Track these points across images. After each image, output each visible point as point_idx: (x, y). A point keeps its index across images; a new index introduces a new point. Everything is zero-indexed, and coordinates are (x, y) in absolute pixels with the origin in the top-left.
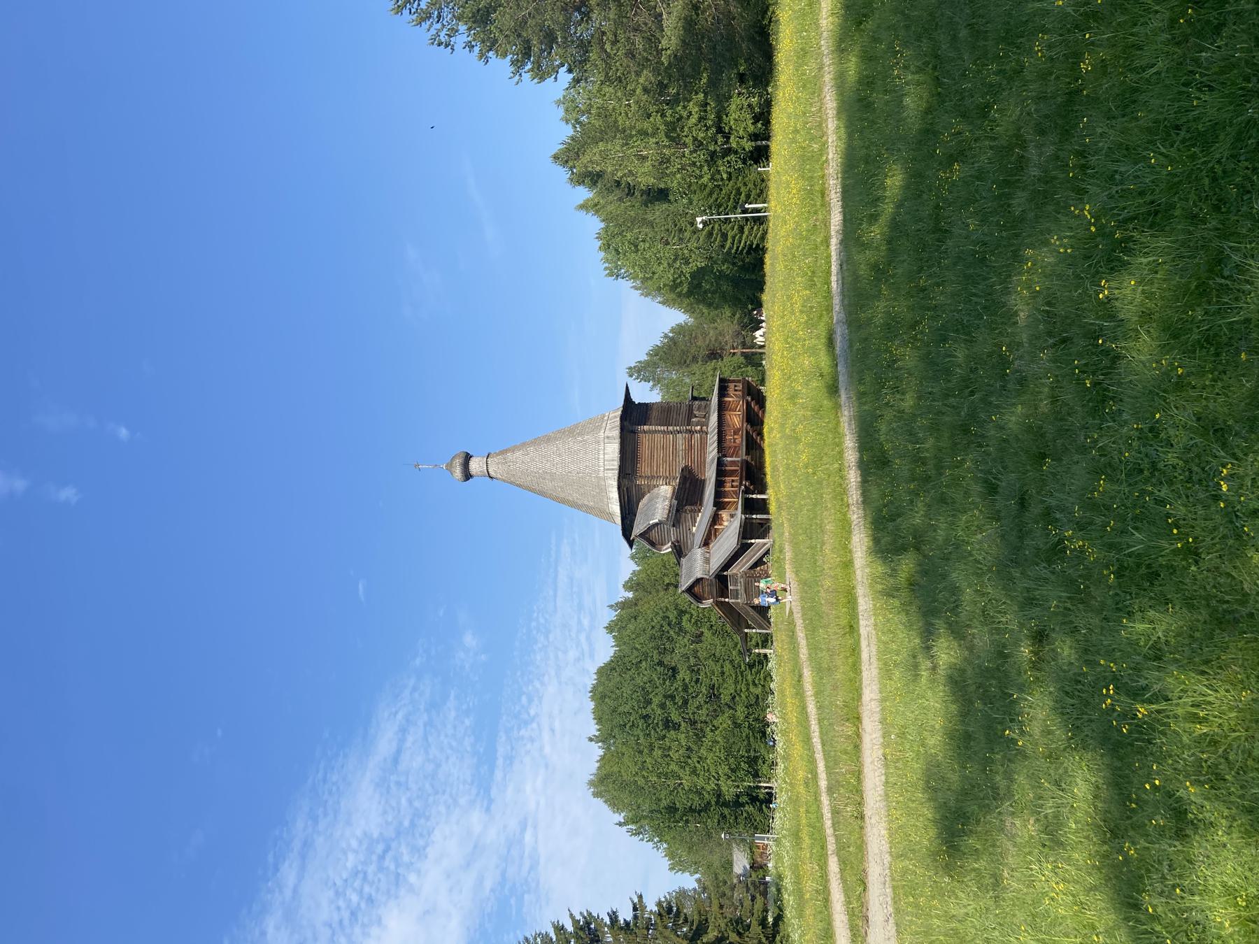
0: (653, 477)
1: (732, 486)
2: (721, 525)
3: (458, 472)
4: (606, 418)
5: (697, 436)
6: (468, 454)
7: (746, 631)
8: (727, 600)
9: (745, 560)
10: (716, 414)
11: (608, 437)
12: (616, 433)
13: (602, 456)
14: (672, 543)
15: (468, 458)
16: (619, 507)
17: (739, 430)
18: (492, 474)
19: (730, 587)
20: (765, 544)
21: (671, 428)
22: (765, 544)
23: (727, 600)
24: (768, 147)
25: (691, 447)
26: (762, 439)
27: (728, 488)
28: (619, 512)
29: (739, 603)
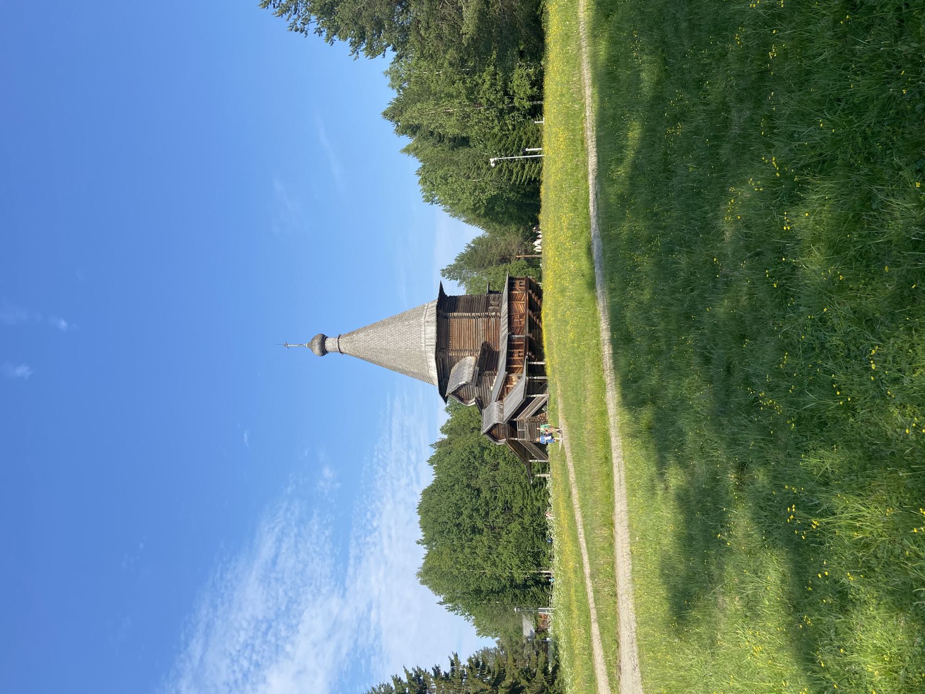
0: (461, 351)
1: (519, 356)
2: (512, 384)
3: (317, 349)
4: (426, 307)
5: (493, 320)
6: (324, 336)
7: (530, 461)
8: (516, 439)
10: (507, 303)
11: (428, 322)
12: (434, 318)
13: (423, 336)
14: (476, 398)
15: (324, 338)
16: (436, 373)
18: (342, 350)
19: (518, 430)
20: (544, 398)
21: (473, 314)
22: (544, 398)
23: (516, 439)
24: (541, 106)
25: (488, 328)
26: (540, 321)
27: (516, 357)
28: (437, 376)
29: (525, 441)
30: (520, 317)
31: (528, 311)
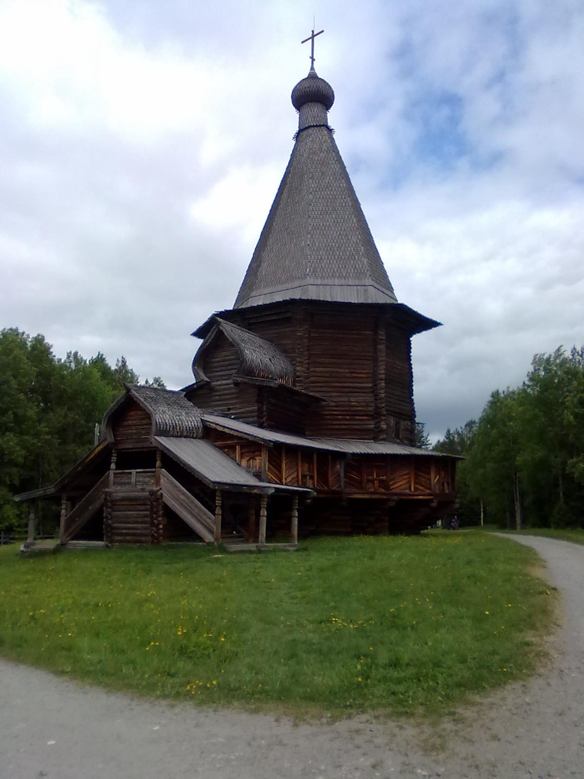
2: (242, 457)
8: (113, 466)
9: (182, 497)
11: (366, 291)
13: (337, 282)
17: (387, 488)
19: (134, 471)
23: (113, 466)
30: (381, 481)
31: (395, 498)
